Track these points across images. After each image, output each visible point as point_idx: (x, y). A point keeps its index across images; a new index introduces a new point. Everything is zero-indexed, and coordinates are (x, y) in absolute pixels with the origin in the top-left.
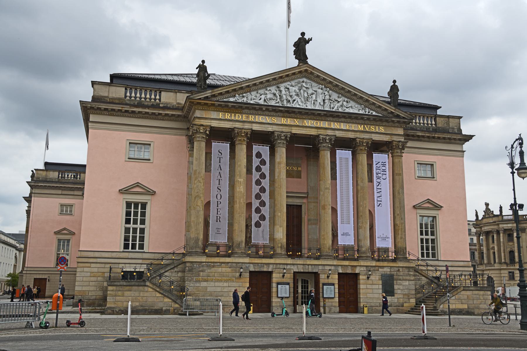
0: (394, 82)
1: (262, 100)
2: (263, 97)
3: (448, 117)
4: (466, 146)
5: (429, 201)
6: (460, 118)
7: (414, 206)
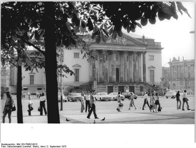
0: (144, 35)
1: (109, 42)
2: (109, 41)
3: (158, 42)
4: (162, 51)
5: (152, 66)
6: (161, 43)
7: (148, 68)
